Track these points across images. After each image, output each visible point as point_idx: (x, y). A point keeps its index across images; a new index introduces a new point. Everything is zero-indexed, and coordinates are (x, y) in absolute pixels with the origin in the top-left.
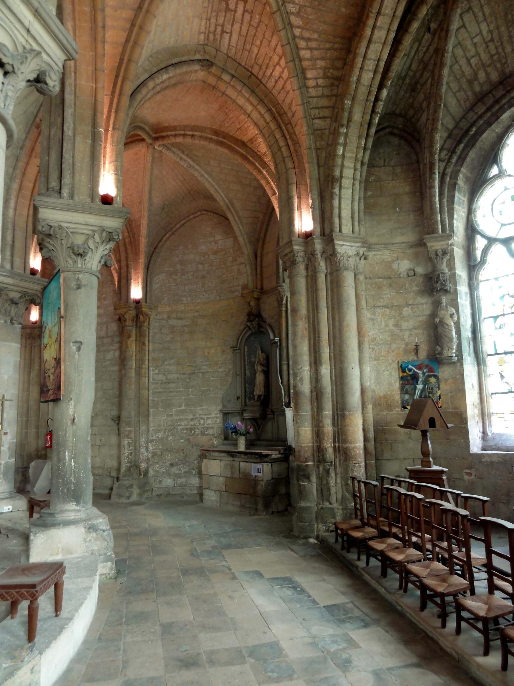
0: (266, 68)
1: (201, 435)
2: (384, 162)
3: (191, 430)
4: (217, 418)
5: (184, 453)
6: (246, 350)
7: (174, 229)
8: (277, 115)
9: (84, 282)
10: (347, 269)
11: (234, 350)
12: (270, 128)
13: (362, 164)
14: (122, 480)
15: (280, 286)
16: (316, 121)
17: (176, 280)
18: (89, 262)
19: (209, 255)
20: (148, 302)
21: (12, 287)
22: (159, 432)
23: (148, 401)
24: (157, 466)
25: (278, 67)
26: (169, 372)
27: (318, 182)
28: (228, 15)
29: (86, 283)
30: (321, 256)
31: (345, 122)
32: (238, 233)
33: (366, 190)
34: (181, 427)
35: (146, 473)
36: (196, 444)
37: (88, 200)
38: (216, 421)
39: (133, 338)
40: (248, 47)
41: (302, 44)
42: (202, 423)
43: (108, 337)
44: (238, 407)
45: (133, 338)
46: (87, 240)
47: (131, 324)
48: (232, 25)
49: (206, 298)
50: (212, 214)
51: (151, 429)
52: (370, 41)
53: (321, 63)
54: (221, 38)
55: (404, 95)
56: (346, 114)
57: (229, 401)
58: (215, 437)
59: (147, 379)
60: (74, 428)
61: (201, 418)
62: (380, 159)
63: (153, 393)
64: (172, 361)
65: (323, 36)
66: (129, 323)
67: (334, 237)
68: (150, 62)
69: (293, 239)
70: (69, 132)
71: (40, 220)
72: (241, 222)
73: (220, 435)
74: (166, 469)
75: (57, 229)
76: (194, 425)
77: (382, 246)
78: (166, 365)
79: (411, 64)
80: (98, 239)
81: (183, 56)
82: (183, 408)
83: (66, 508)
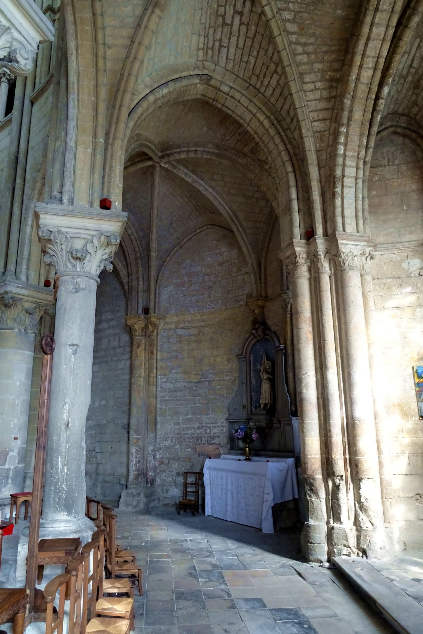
0: (264, 77)
1: (208, 443)
2: (389, 161)
3: (197, 438)
4: (223, 426)
5: (190, 462)
6: (252, 358)
7: (182, 244)
8: (275, 122)
9: (82, 286)
10: (352, 268)
11: (240, 358)
12: (269, 134)
13: (365, 163)
14: (130, 488)
15: (285, 293)
16: (316, 124)
17: (184, 291)
18: (88, 266)
19: (215, 267)
20: (156, 313)
21: (27, 298)
22: (166, 440)
23: (156, 409)
24: (165, 474)
25: (275, 75)
26: (177, 381)
27: (319, 182)
28: (225, 29)
29: (84, 287)
30: (325, 257)
31: (345, 121)
32: (242, 243)
33: (370, 189)
34: (187, 436)
35: (153, 481)
36: (202, 454)
37: (87, 205)
38: (222, 430)
39: (142, 347)
40: (245, 59)
41: (300, 49)
42: (208, 431)
43: (120, 347)
45: (142, 347)
46: (86, 244)
47: (140, 334)
48: (229, 39)
49: (212, 308)
50: (217, 228)
51: (158, 437)
52: (368, 39)
53: (318, 66)
54: (219, 53)
55: (406, 94)
56: (346, 114)
57: (236, 409)
58: (221, 447)
59: (155, 387)
60: (68, 433)
61: (207, 427)
62: (384, 158)
63: (161, 401)
64: (179, 370)
65: (319, 40)
66: (138, 332)
67: (337, 236)
68: (151, 78)
69: (294, 240)
70: (71, 144)
71: (41, 226)
72: (245, 233)
73: (226, 444)
74: (173, 478)
75: (57, 234)
76: (201, 434)
77: (390, 245)
78: (174, 374)
79: (412, 61)
80: (97, 242)
81: (182, 72)
82: (190, 416)
83: (56, 518)
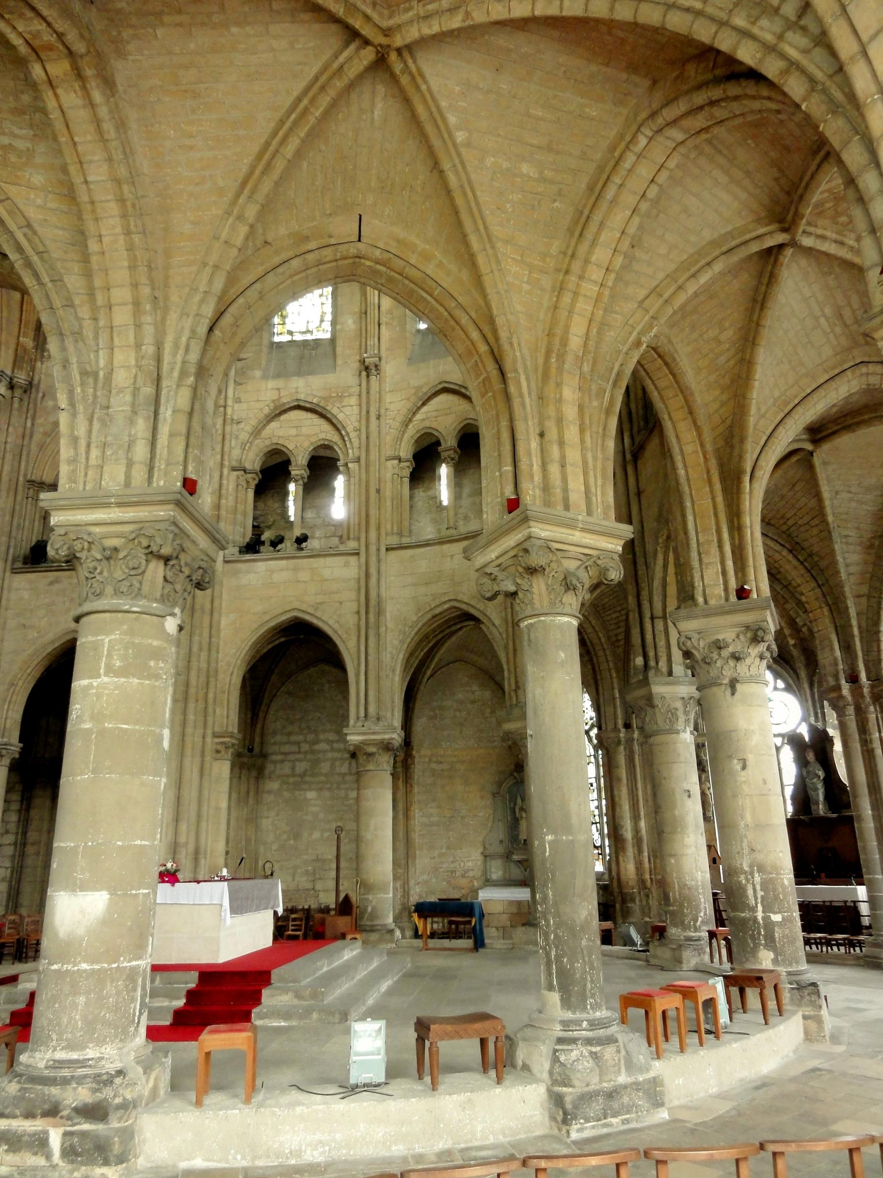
3: (452, 872)
43: (351, 774)
44: (500, 850)
